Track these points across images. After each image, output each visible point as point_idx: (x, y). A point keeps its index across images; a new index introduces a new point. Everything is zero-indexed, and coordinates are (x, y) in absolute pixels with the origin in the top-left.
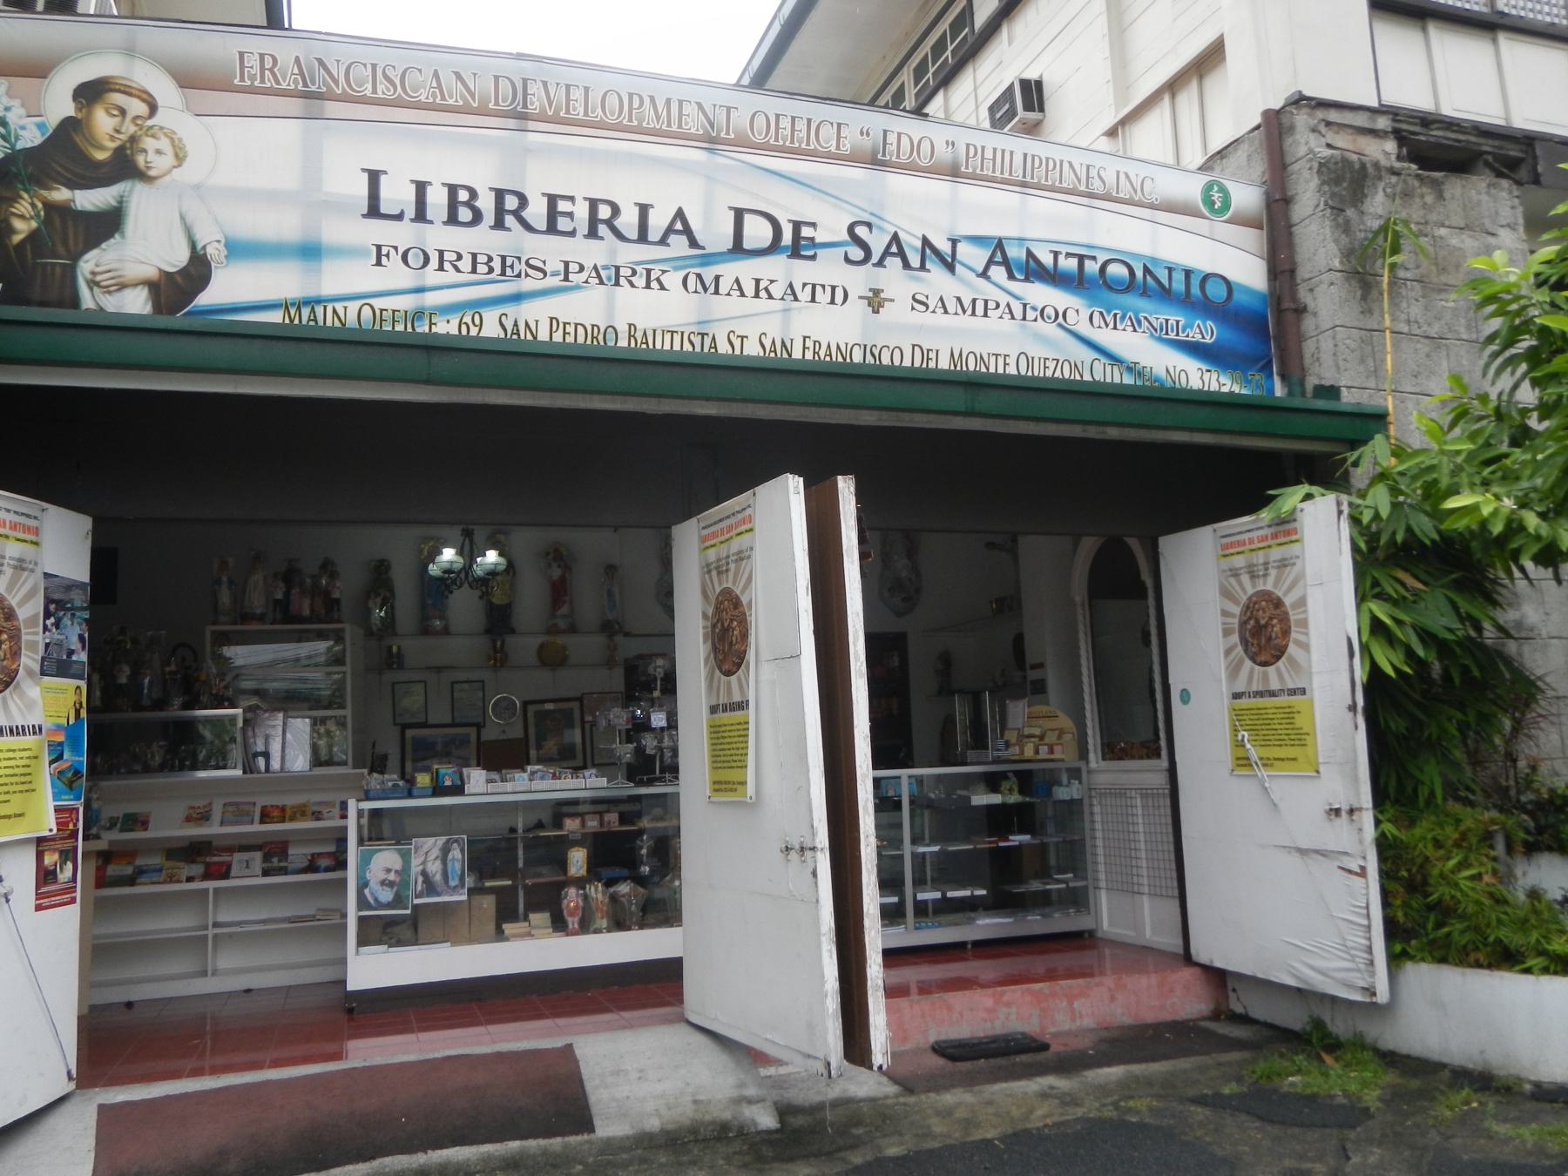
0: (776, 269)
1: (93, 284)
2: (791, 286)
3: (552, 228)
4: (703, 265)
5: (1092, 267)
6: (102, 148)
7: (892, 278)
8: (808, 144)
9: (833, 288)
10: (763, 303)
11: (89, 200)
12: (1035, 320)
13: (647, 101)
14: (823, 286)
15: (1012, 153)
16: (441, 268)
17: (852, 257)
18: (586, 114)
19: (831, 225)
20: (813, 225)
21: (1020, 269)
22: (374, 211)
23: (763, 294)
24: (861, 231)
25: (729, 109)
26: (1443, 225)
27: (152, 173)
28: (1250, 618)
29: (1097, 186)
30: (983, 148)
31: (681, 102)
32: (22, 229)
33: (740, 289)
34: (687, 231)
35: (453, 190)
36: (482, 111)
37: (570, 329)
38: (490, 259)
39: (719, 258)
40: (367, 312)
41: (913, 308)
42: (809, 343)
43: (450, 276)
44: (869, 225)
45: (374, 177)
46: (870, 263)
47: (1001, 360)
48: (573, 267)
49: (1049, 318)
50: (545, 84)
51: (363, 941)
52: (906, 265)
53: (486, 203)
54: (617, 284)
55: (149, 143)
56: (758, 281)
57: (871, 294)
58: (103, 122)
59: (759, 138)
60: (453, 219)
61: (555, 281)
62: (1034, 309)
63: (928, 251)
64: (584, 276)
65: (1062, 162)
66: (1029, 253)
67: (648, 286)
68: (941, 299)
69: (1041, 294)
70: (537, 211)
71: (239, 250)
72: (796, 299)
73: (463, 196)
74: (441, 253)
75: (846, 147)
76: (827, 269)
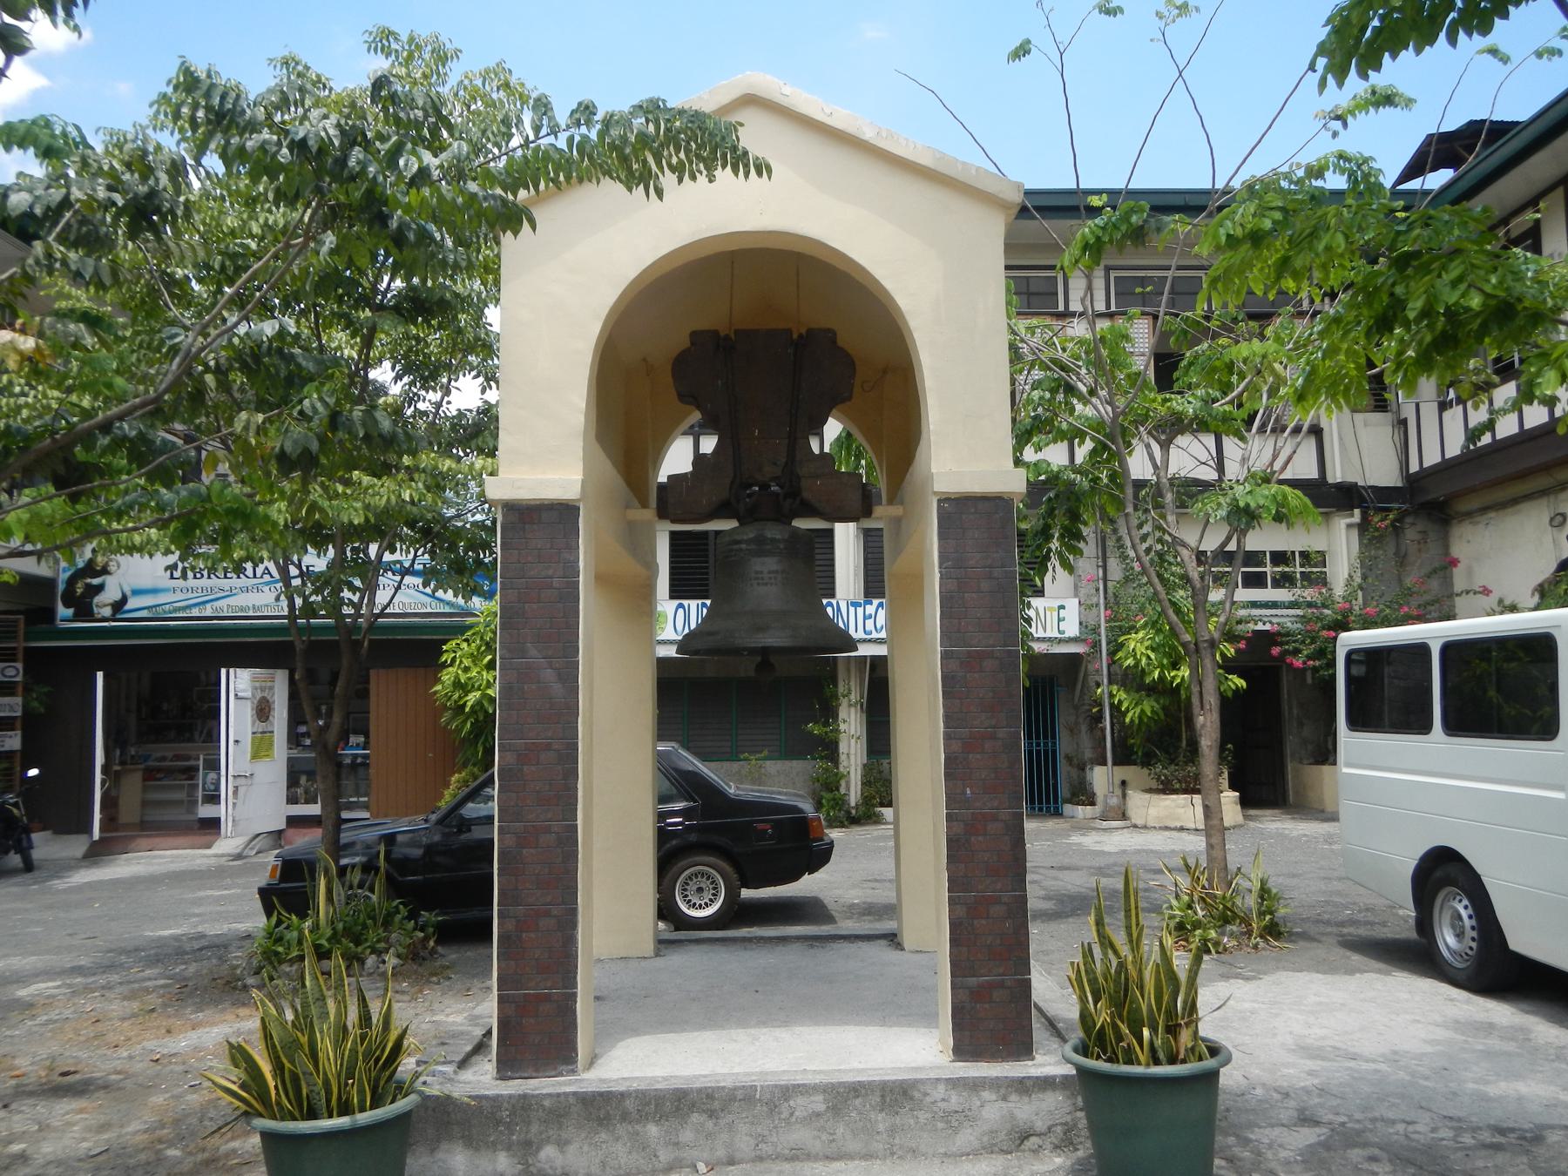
11: (96, 581)
32: (79, 591)
51: (203, 803)
60: (195, 577)
71: (136, 592)
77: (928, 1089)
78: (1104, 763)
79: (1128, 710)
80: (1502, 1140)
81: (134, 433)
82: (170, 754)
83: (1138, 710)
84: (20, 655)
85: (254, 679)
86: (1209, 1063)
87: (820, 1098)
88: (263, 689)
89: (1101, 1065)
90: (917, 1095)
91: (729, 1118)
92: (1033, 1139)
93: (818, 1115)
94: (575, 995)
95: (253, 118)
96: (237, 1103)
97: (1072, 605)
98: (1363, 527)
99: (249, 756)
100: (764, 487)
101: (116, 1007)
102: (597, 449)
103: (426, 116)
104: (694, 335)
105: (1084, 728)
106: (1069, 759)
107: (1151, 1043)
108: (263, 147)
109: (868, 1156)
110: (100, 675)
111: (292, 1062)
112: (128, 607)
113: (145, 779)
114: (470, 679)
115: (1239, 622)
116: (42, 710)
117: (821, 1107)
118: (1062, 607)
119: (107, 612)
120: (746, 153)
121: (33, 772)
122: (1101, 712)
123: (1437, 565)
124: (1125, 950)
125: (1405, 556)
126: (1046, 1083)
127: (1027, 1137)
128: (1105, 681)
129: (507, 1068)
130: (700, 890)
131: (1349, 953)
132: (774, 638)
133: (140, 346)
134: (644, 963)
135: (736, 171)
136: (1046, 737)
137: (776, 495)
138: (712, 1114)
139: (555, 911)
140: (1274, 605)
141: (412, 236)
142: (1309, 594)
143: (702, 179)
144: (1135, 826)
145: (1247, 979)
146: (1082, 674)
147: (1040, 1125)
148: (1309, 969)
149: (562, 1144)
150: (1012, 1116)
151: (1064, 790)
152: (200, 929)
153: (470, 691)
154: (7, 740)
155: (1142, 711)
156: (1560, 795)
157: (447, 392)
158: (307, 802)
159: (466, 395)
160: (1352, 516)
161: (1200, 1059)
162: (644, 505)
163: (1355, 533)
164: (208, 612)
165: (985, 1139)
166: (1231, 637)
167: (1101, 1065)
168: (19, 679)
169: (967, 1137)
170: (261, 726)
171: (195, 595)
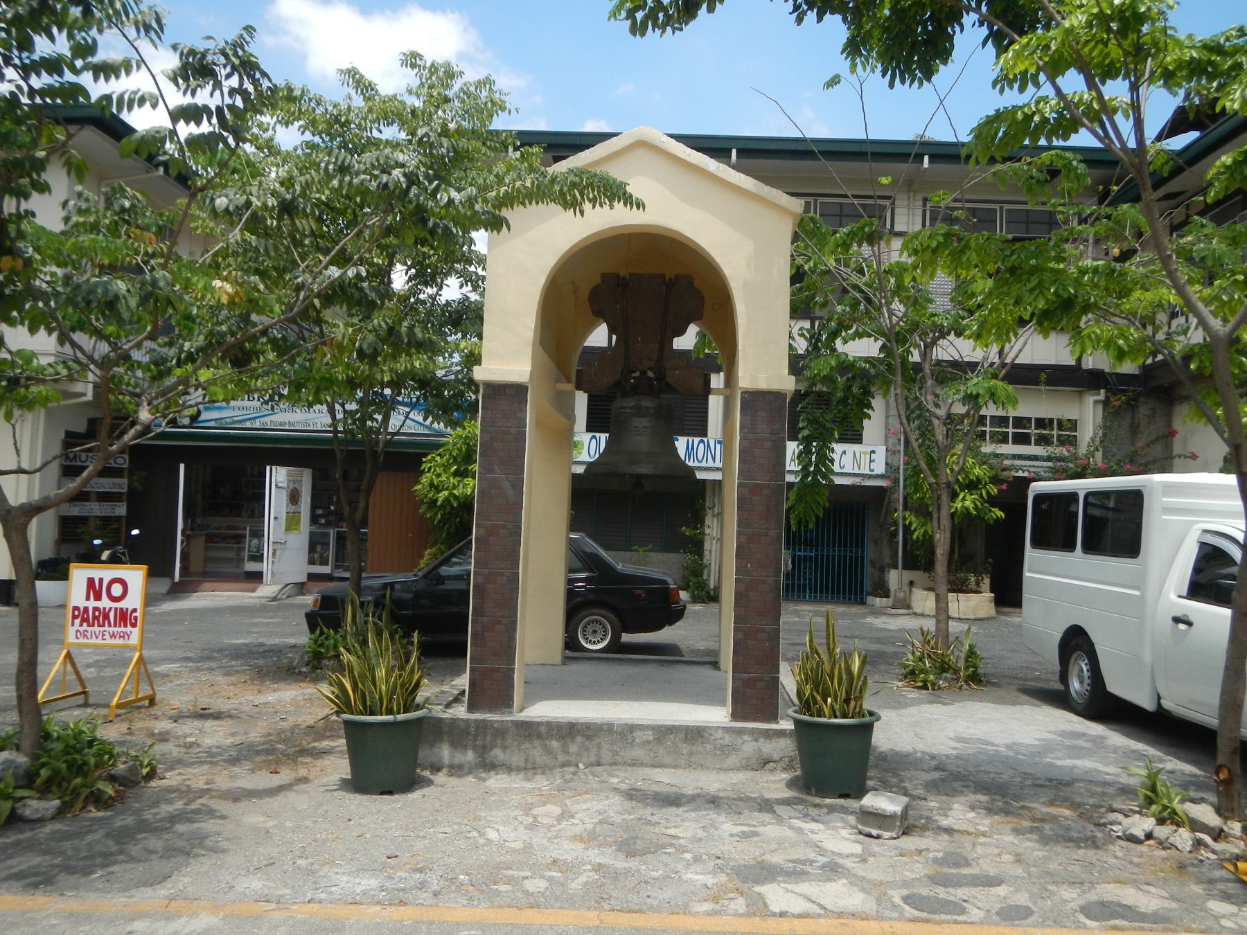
10: (321, 415)
51: (248, 560)
77: (712, 731)
78: (896, 568)
79: (915, 530)
80: (1048, 783)
81: (280, 336)
82: (225, 525)
83: (922, 530)
85: (289, 475)
86: (868, 719)
87: (650, 733)
88: (294, 482)
89: (806, 718)
90: (706, 735)
91: (598, 740)
92: (771, 764)
93: (649, 742)
94: (514, 669)
95: (359, 169)
96: (333, 706)
97: (881, 451)
98: (1106, 403)
99: (284, 529)
100: (643, 373)
101: (221, 679)
102: (541, 350)
103: (448, 151)
104: (604, 276)
105: (885, 541)
106: (873, 563)
107: (832, 706)
108: (362, 182)
109: (675, 767)
110: (182, 466)
111: (364, 686)
112: (201, 419)
113: (207, 542)
114: (441, 482)
115: (1004, 470)
116: (141, 488)
117: (651, 738)
118: (873, 452)
120: (631, 196)
121: (135, 532)
122: (897, 530)
123: (1161, 434)
124: (825, 657)
125: (1138, 427)
126: (781, 733)
127: (768, 763)
128: (901, 508)
129: (472, 708)
130: (595, 632)
131: (1021, 695)
132: (643, 469)
133: (250, 260)
134: (554, 667)
135: (625, 204)
136: (857, 547)
137: (651, 378)
138: (589, 738)
139: (504, 621)
140: (1035, 458)
141: (440, 231)
142: (1063, 451)
143: (606, 207)
144: (915, 614)
145: (945, 704)
146: (885, 504)
147: (776, 756)
148: (989, 701)
149: (504, 748)
150: (760, 750)
151: (867, 586)
152: (260, 640)
153: (440, 491)
154: (117, 508)
155: (926, 531)
156: (1137, 593)
157: (441, 288)
158: (321, 564)
159: (452, 290)
160: (1099, 394)
161: (863, 717)
162: (569, 381)
163: (1100, 408)
164: (257, 424)
165: (744, 762)
166: (995, 480)
167: (806, 718)
168: (126, 466)
169: (733, 760)
170: (292, 508)
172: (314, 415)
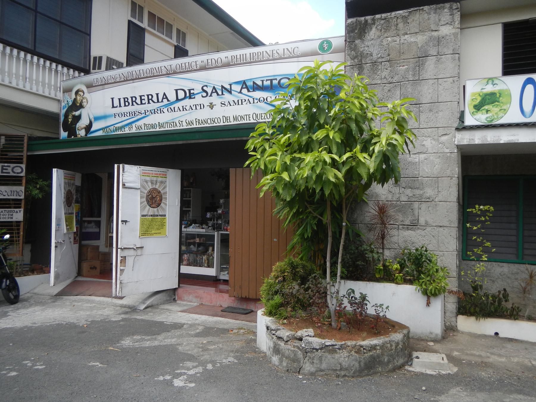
0: (187, 102)
1: (78, 129)
2: (190, 106)
3: (142, 103)
4: (170, 105)
5: (275, 82)
6: (78, 103)
7: (215, 99)
8: (189, 69)
9: (200, 105)
10: (185, 112)
11: (77, 113)
12: (257, 102)
13: (154, 69)
14: (198, 105)
15: (246, 54)
16: (125, 116)
17: (203, 96)
18: (144, 76)
19: (198, 88)
20: (193, 89)
21: (251, 89)
22: (113, 107)
23: (185, 110)
24: (205, 88)
25: (171, 65)
26: (407, 34)
27: (84, 106)
28: (150, 195)
29: (276, 55)
30: (236, 56)
31: (161, 67)
33: (179, 109)
34: (167, 98)
35: (124, 99)
36: (127, 80)
37: (148, 126)
38: (132, 113)
39: (174, 103)
40: (114, 128)
41: (221, 106)
42: (197, 120)
43: (126, 118)
44: (206, 86)
45: (112, 99)
46: (208, 96)
47: (248, 116)
48: (146, 111)
49: (262, 101)
50: (135, 71)
52: (218, 94)
53: (130, 101)
54: (155, 113)
55: (84, 101)
56: (183, 107)
57: (210, 104)
58: (78, 98)
59: (178, 71)
60: (125, 106)
61: (144, 115)
62: (257, 99)
63: (223, 89)
64: (149, 112)
65: (263, 52)
66: (253, 82)
67: (161, 113)
68: (229, 102)
69: (258, 94)
70: (138, 101)
71: (97, 119)
72: (192, 109)
73: (126, 100)
74: (124, 113)
75: (198, 67)
76: (199, 100)
84: (25, 160)
85: (144, 174)
99: (138, 233)
112: (93, 129)
116: (40, 196)
119: (82, 133)
121: (7, 236)
154: (14, 214)
164: (134, 130)
171: (126, 118)
172: (178, 114)
